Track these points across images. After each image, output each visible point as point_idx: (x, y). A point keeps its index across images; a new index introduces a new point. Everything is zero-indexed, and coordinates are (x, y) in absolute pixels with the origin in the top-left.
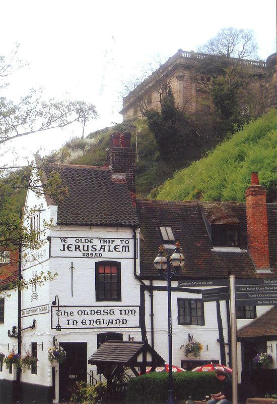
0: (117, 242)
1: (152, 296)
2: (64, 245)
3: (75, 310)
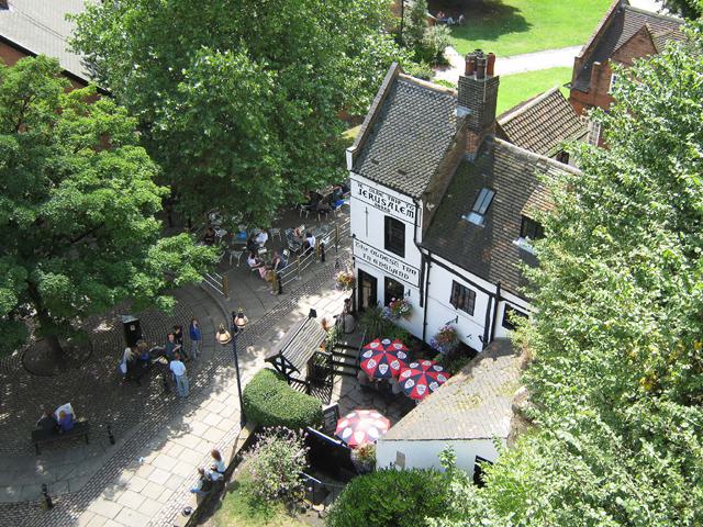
0: (403, 204)
1: (430, 267)
3: (370, 249)
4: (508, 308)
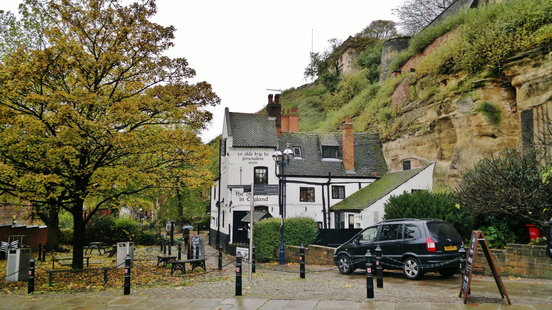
4: (332, 186)
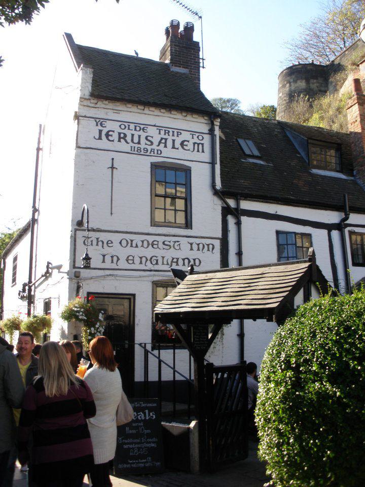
0: (185, 136)
1: (238, 224)
2: (100, 131)
3: (116, 238)
4: (351, 233)
